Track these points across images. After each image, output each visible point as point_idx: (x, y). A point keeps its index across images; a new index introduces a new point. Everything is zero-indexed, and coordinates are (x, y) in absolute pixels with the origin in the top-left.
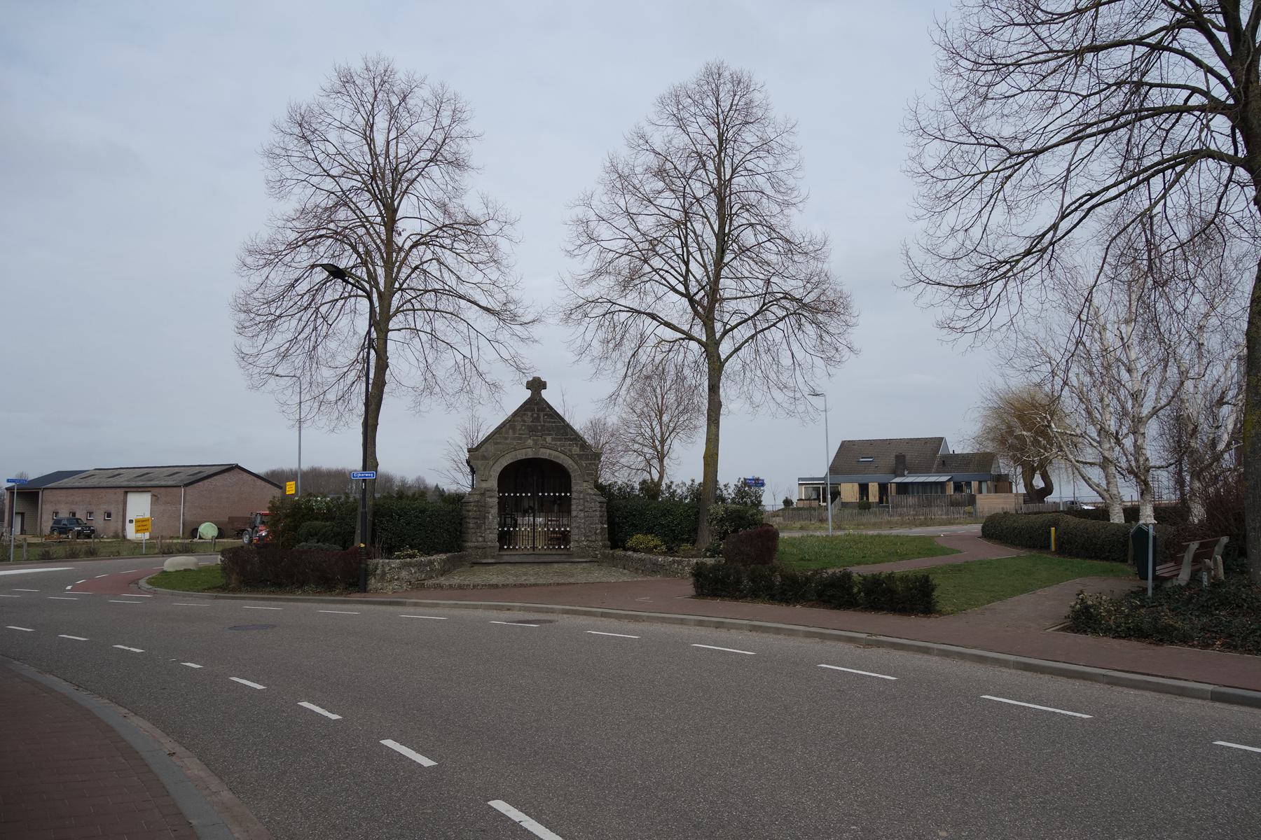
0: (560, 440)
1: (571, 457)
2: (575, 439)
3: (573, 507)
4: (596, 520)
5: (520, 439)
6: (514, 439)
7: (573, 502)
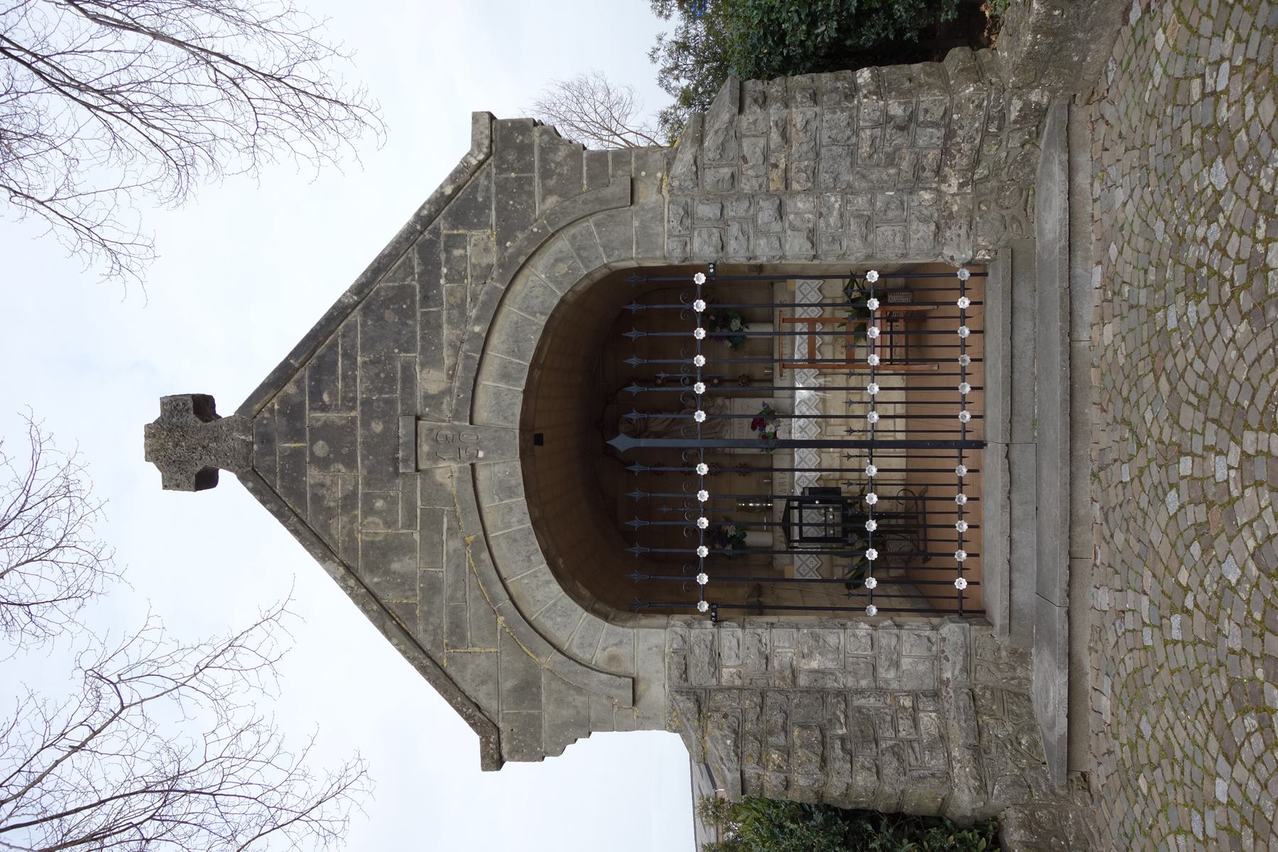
0: (432, 326)
1: (514, 271)
2: (428, 251)
3: (764, 251)
4: (833, 120)
5: (432, 520)
6: (433, 547)
7: (737, 253)
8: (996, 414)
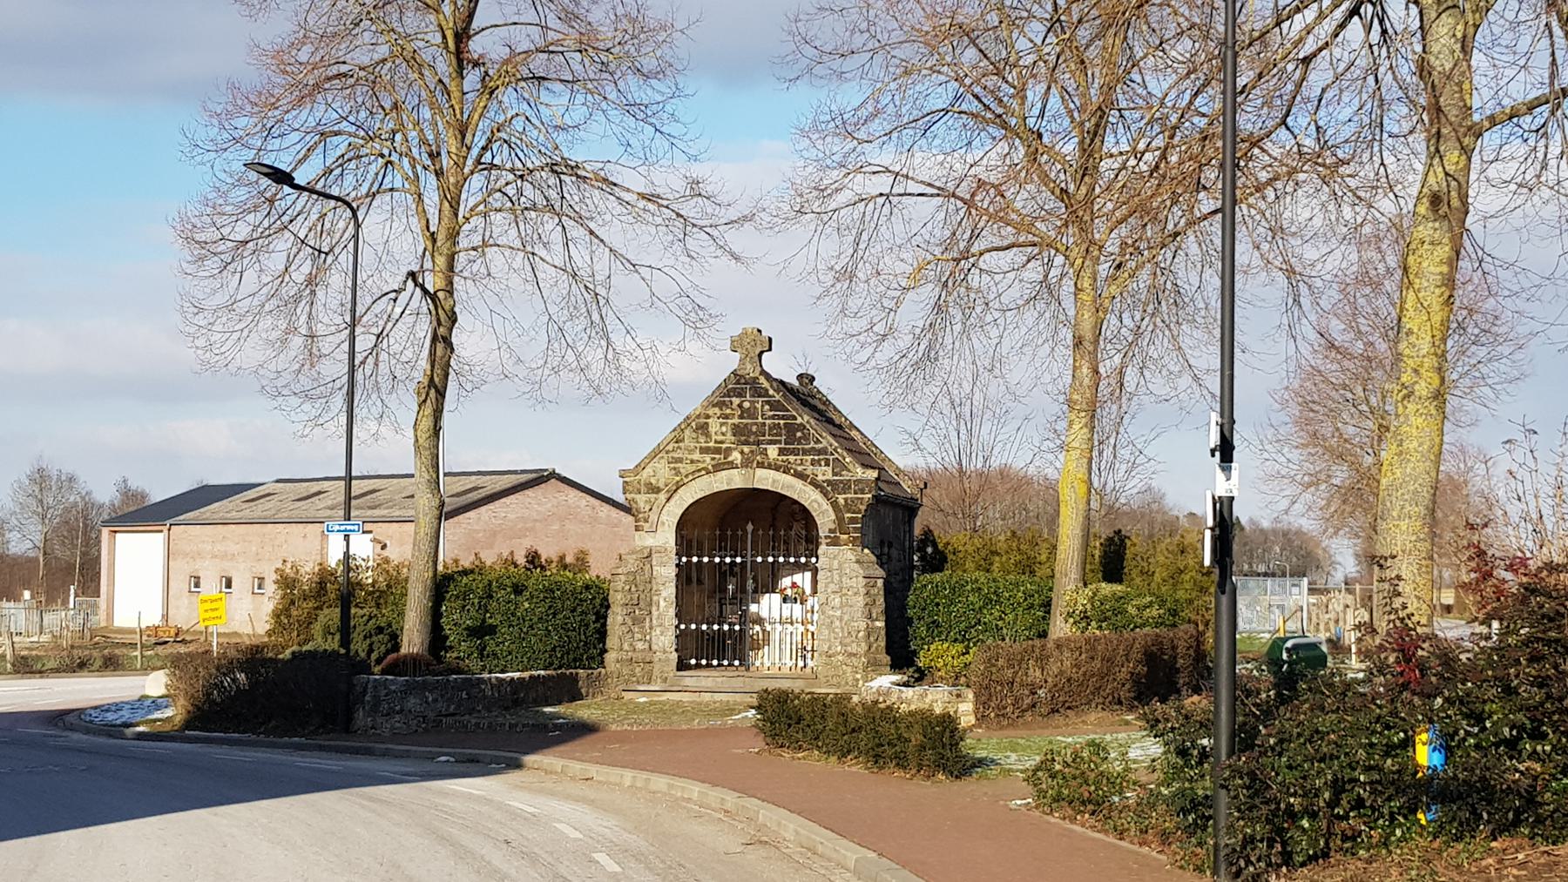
1: (815, 484)
8: (758, 674)
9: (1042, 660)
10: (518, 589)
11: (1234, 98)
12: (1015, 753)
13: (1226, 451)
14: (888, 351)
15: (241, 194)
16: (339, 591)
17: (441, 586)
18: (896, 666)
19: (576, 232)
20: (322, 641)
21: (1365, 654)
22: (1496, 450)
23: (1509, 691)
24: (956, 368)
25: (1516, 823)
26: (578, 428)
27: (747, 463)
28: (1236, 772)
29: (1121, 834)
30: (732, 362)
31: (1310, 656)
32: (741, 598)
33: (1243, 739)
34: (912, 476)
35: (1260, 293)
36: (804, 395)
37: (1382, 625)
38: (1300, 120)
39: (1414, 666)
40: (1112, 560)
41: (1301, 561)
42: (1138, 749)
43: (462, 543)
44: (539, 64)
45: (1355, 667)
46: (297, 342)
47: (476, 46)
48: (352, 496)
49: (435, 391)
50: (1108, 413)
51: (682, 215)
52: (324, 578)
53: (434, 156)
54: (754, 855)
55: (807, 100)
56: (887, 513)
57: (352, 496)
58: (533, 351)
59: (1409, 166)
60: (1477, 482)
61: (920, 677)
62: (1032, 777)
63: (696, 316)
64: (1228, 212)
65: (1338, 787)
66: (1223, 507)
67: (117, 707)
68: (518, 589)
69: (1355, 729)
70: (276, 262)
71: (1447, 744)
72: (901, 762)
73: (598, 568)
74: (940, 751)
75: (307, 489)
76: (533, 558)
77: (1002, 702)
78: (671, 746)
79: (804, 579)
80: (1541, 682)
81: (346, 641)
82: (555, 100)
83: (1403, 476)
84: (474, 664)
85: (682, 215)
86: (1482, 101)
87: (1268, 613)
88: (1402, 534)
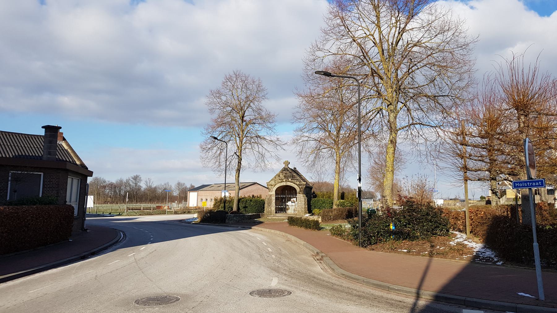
9: (332, 212)
10: (251, 201)
11: (360, 126)
12: (328, 226)
13: (360, 180)
14: (307, 164)
15: (209, 141)
16: (224, 201)
17: (239, 200)
18: (309, 213)
19: (260, 146)
20: (221, 209)
21: (382, 211)
22: (402, 179)
23: (405, 217)
24: (318, 166)
25: (406, 238)
26: (260, 176)
27: (286, 181)
28: (362, 230)
29: (344, 239)
30: (284, 166)
31: (373, 212)
32: (285, 202)
33: (363, 225)
34: (311, 183)
35: (365, 155)
36: (295, 171)
37: (385, 207)
38: (370, 129)
39: (390, 213)
40: (342, 196)
41: (371, 196)
42: (347, 226)
43: (245, 193)
44: (254, 121)
45: (380, 213)
46: (218, 163)
47: (245, 119)
48: (226, 187)
49: (238, 170)
50: (342, 174)
51: (275, 143)
52: (221, 199)
53: (239, 135)
54: (287, 242)
55: (296, 125)
56: (308, 189)
57: (226, 187)
58: (253, 164)
59: (387, 136)
60: (399, 184)
61: (313, 214)
62: (330, 230)
63: (278, 159)
64: (359, 143)
65: (378, 232)
66: (360, 189)
67: (190, 219)
68: (251, 201)
69: (381, 223)
70: (214, 151)
71: (395, 225)
72: (310, 228)
73: (263, 198)
74: (316, 226)
75: (219, 185)
76: (253, 196)
77: (326, 218)
78: (274, 225)
79: (295, 199)
80: (410, 216)
81: (225, 209)
82: (257, 126)
83: (387, 183)
84: (244, 212)
85: (275, 143)
86: (398, 126)
87: (367, 204)
88: (387, 192)
